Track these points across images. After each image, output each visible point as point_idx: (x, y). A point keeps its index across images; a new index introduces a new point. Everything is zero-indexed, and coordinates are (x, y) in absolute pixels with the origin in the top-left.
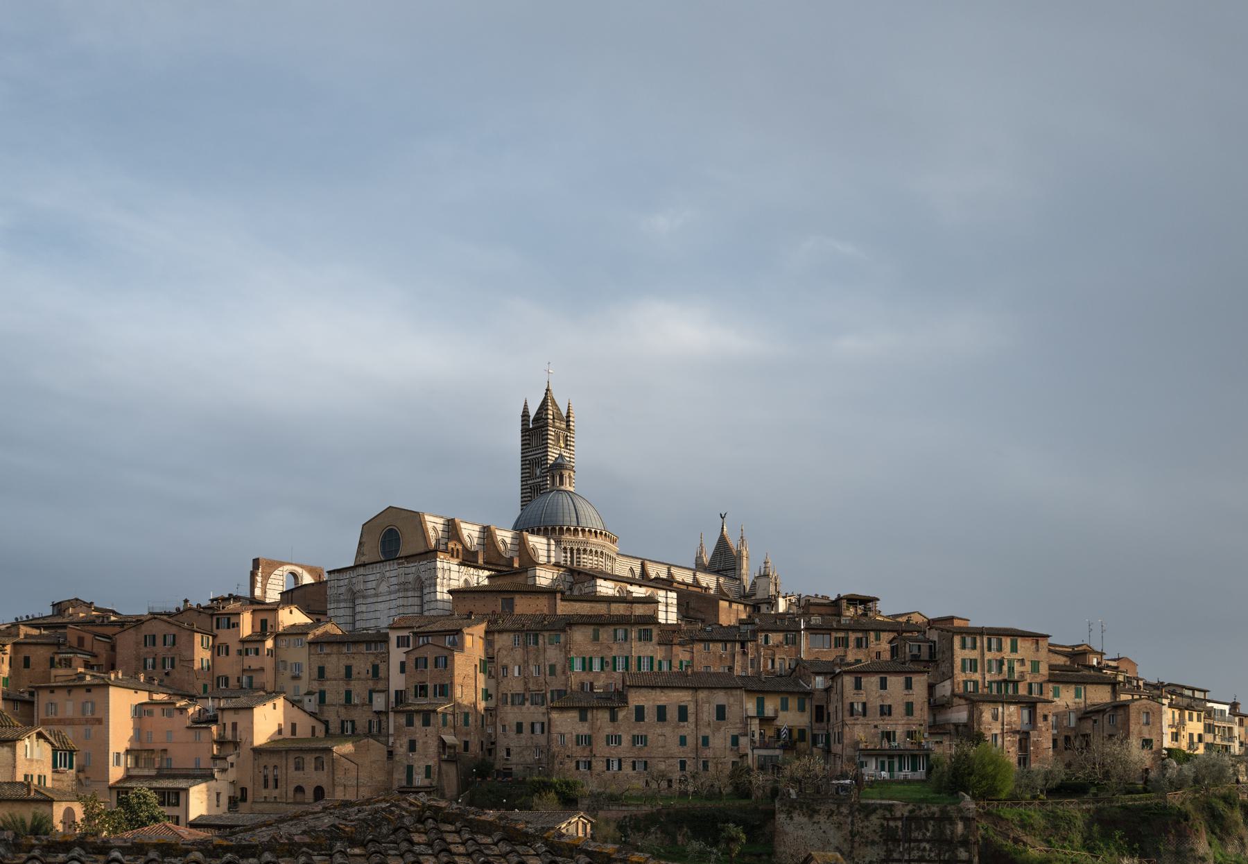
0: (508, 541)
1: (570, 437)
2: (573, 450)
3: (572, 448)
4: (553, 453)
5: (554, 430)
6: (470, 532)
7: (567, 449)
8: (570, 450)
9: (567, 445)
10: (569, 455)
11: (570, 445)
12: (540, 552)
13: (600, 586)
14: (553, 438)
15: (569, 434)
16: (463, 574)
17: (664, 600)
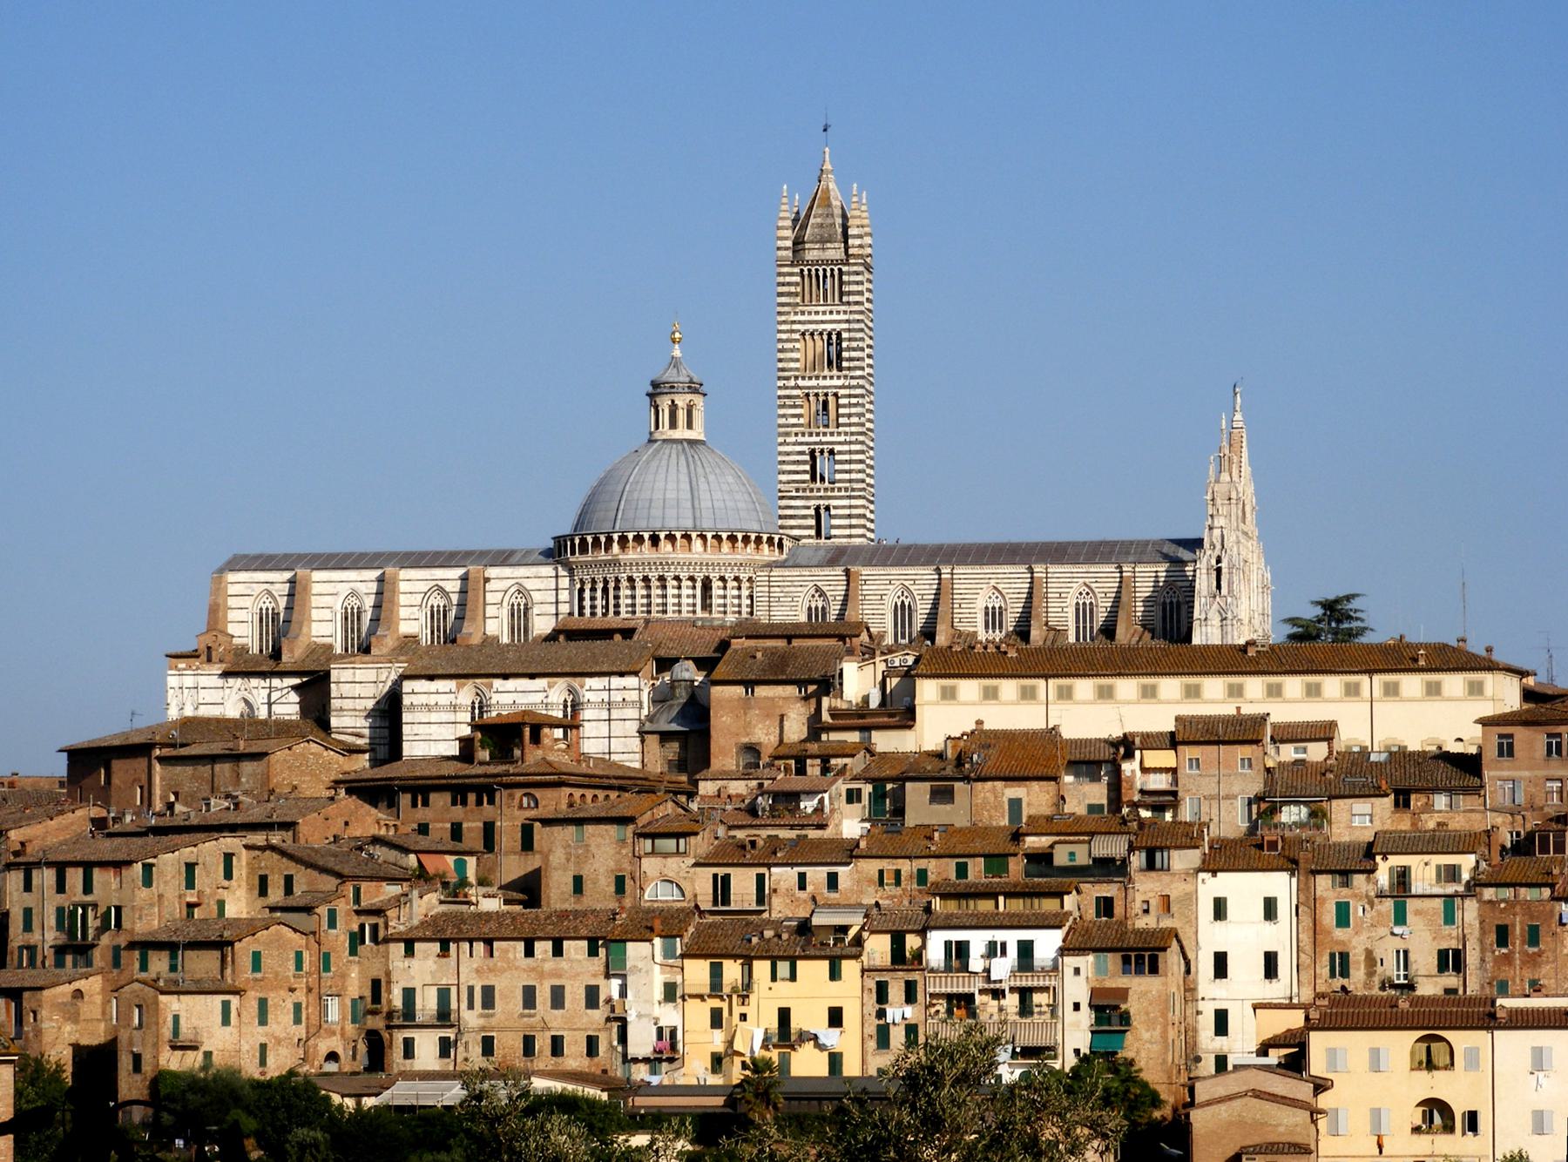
0: (449, 587)
1: (849, 273)
2: (857, 303)
3: (852, 298)
4: (794, 322)
5: (797, 270)
6: (352, 585)
7: (843, 303)
8: (849, 303)
9: (841, 294)
10: (842, 317)
11: (849, 293)
12: (536, 596)
13: (413, 693)
14: (792, 289)
15: (845, 269)
16: (235, 690)
17: (605, 695)
